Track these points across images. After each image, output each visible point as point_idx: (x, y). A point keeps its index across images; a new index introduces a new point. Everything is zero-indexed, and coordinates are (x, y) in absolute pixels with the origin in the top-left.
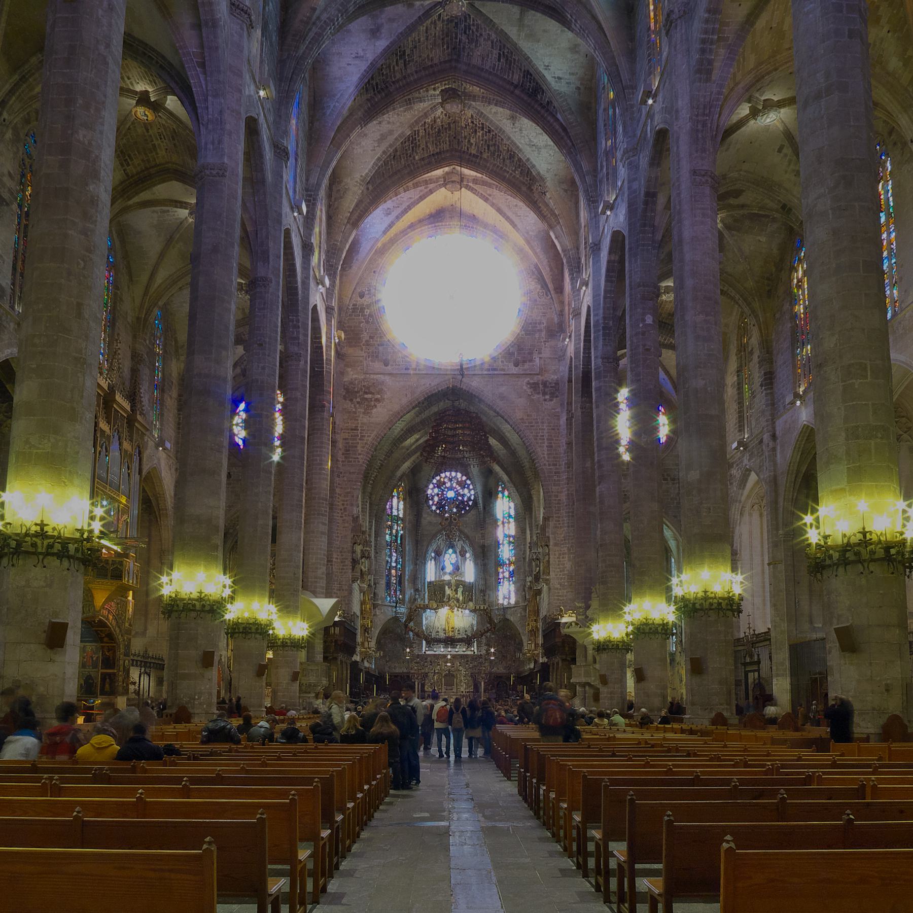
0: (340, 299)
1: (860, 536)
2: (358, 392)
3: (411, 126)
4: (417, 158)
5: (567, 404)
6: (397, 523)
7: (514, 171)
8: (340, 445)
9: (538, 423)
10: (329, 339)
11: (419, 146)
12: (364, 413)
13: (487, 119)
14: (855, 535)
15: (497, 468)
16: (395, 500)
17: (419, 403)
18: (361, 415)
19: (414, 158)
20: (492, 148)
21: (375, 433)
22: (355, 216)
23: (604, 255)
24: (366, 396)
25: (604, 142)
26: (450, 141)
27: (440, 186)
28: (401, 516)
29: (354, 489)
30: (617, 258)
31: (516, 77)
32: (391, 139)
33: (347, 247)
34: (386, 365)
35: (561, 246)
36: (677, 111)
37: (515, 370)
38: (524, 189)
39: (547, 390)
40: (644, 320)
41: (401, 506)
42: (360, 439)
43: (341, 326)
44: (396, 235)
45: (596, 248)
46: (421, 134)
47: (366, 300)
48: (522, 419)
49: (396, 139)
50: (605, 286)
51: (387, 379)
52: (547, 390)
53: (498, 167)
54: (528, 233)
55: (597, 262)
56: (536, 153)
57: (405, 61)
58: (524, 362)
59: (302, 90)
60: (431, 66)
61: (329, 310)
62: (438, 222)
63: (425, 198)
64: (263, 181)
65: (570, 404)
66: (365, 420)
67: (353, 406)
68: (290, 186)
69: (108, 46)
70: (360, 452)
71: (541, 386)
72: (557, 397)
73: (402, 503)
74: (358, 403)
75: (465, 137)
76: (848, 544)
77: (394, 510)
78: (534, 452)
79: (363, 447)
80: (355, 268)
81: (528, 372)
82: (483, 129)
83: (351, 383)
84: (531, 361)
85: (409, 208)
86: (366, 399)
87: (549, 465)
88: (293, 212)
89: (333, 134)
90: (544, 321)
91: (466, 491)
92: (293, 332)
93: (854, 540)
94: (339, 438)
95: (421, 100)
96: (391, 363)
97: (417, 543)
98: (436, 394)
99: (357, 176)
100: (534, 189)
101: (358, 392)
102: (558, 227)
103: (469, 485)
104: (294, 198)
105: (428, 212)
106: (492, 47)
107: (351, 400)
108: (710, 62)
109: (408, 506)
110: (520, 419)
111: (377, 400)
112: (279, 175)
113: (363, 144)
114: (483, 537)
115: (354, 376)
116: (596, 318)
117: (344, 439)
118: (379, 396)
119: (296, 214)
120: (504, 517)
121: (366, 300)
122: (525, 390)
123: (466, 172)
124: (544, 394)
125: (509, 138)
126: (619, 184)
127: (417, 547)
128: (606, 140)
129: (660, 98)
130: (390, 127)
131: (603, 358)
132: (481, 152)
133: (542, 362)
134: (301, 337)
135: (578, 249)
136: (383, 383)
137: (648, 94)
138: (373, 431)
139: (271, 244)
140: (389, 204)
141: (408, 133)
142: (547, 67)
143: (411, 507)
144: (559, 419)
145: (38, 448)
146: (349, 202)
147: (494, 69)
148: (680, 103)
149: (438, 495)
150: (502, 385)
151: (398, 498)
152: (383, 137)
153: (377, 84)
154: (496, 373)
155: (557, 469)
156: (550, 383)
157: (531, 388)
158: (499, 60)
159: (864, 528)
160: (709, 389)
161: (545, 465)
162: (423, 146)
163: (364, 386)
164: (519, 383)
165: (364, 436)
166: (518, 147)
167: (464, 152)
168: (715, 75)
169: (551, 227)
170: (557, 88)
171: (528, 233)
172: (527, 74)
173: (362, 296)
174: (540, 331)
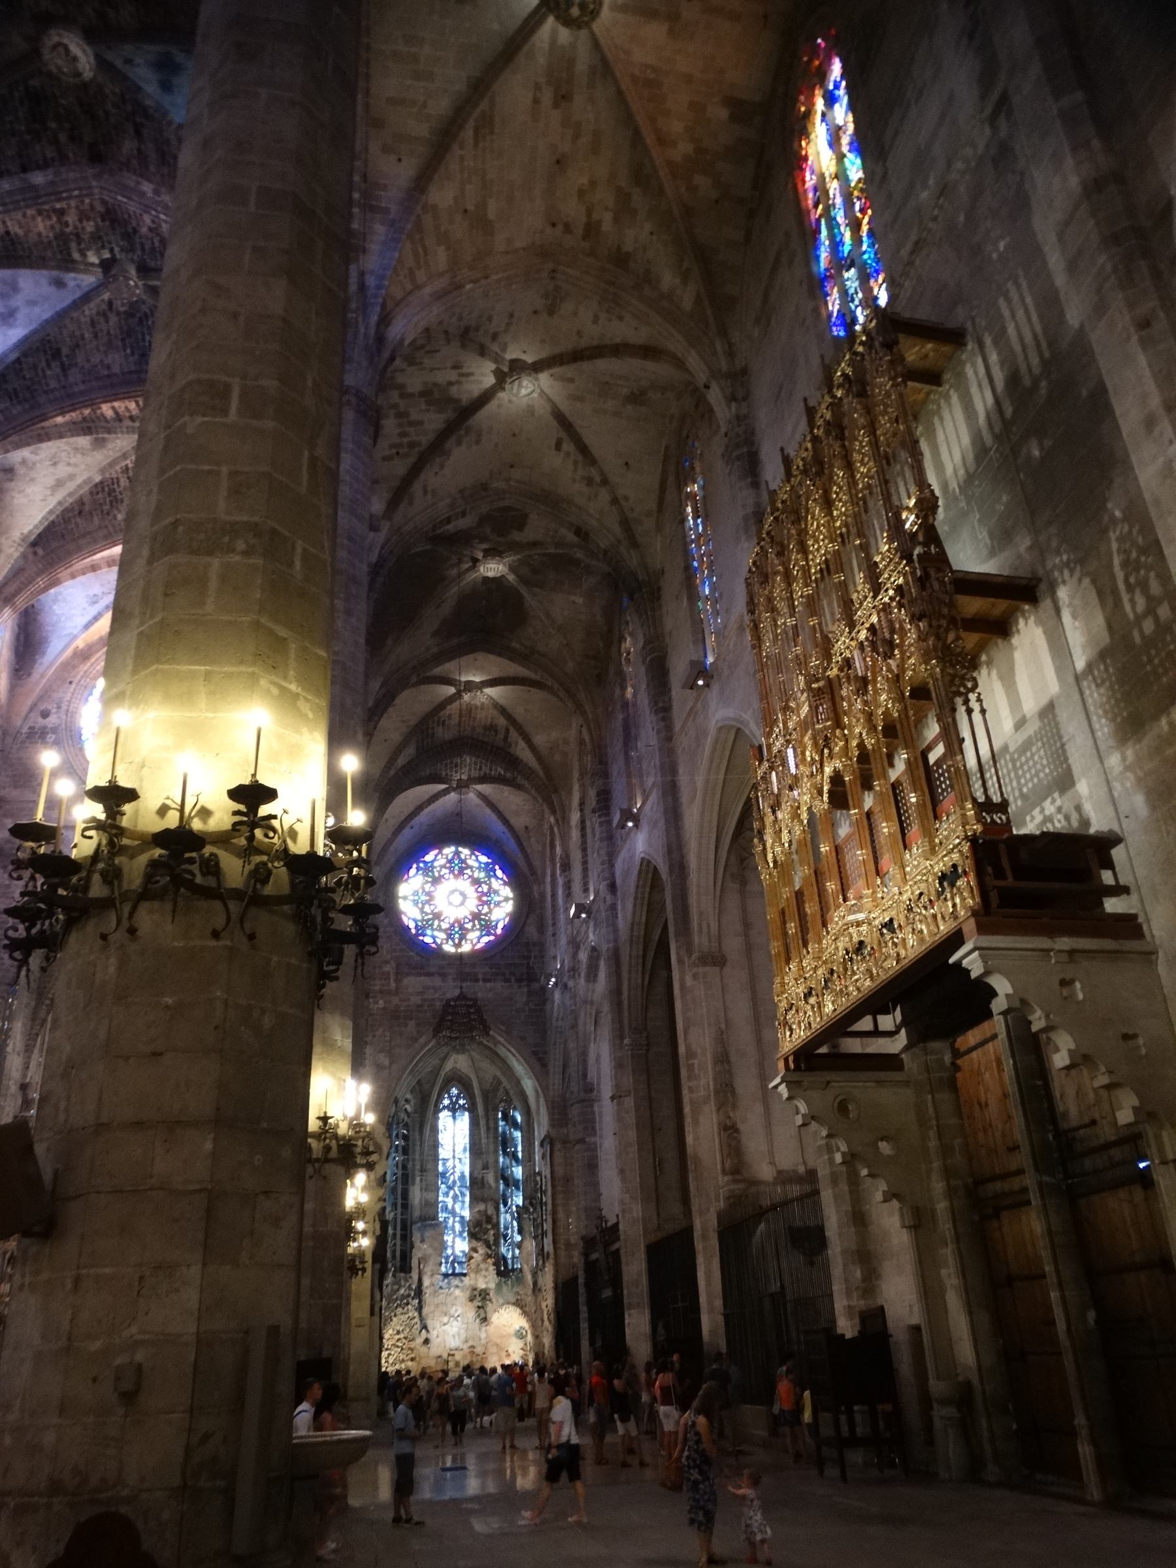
32: (71, 486)
47: (52, 720)
80: (36, 675)
99: (16, 535)
113: (29, 491)
130: (70, 470)
152: (59, 484)
173: (45, 714)
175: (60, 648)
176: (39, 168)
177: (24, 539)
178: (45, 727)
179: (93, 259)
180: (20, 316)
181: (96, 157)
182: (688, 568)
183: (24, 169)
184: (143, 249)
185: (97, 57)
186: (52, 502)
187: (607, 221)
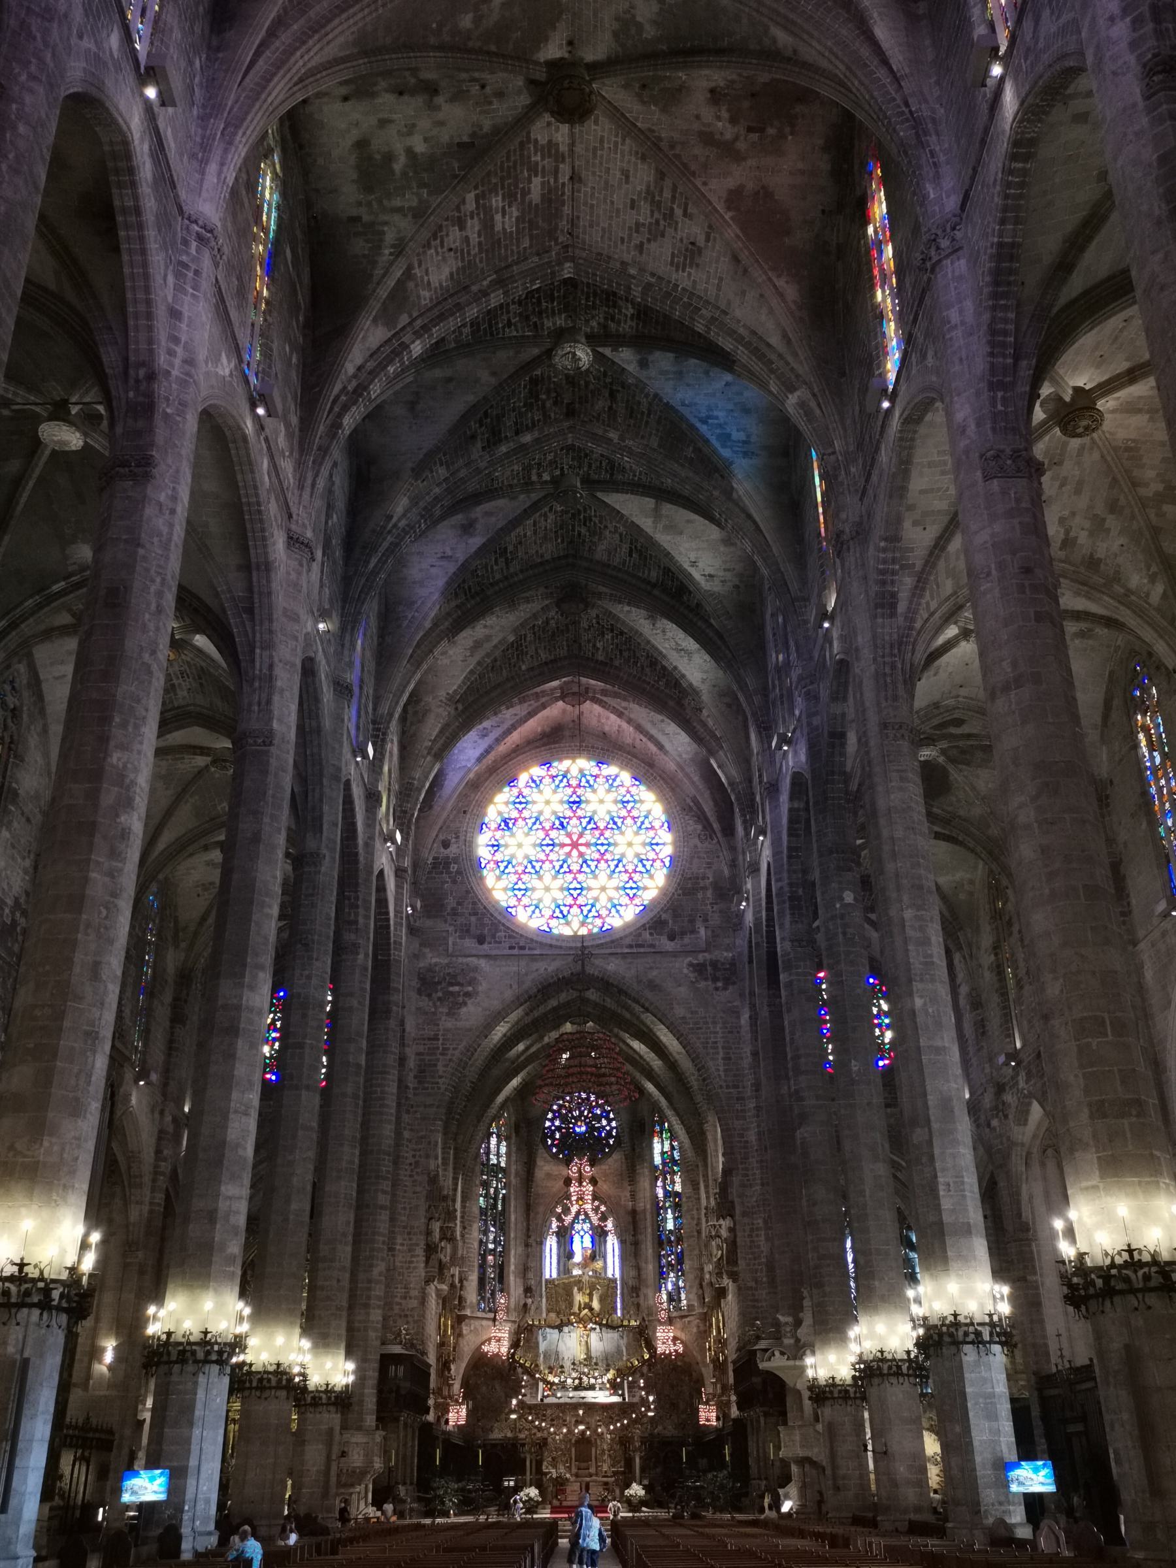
0: (416, 850)
1: (1126, 1256)
2: (439, 983)
3: (515, 631)
4: (524, 667)
5: (750, 994)
6: (496, 1177)
7: (657, 682)
8: (411, 1063)
9: (707, 1023)
10: (398, 912)
11: (527, 653)
12: (448, 1014)
13: (618, 619)
14: (1119, 1253)
15: (650, 1087)
16: (494, 1141)
17: (530, 997)
18: (443, 1018)
19: (520, 668)
20: (626, 654)
21: (464, 1043)
22: (438, 745)
23: (784, 797)
24: (451, 989)
25: (774, 655)
26: (568, 646)
27: (557, 699)
28: (503, 1165)
29: (431, 1131)
30: (802, 805)
31: (654, 574)
32: (488, 646)
33: (427, 785)
34: (481, 940)
35: (727, 778)
36: (857, 650)
37: (669, 946)
38: (671, 703)
39: (718, 974)
40: (841, 899)
41: (503, 1150)
42: (442, 1054)
43: (416, 891)
44: (494, 761)
45: (773, 789)
46: (528, 639)
47: (453, 850)
48: (684, 1018)
49: (495, 647)
50: (789, 842)
51: (482, 963)
52: (718, 974)
53: (635, 676)
54: (680, 756)
55: (775, 807)
56: (686, 660)
57: (507, 559)
58: (683, 933)
59: (371, 608)
60: (541, 564)
61: (399, 872)
62: (555, 743)
63: (536, 714)
64: (319, 730)
65: (752, 994)
66: (449, 1025)
67: (431, 1004)
68: (353, 732)
69: (153, 653)
70: (440, 1073)
72: (734, 983)
73: (504, 1143)
74: (439, 999)
75: (589, 641)
76: (1113, 1265)
79: (446, 1066)
80: (436, 809)
81: (689, 948)
82: (612, 631)
83: (430, 969)
85: (514, 727)
86: (452, 993)
87: (728, 1087)
88: (356, 756)
89: (411, 651)
90: (710, 875)
91: (604, 1122)
92: (349, 914)
93: (1119, 1260)
94: (410, 1052)
95: (527, 600)
96: (488, 939)
97: (528, 1209)
98: (554, 983)
99: (442, 694)
100: (686, 702)
101: (439, 983)
102: (721, 753)
103: (608, 1113)
104: (357, 737)
105: (539, 729)
106: (621, 541)
107: (429, 996)
108: (894, 595)
109: (514, 1149)
111: (468, 995)
112: (339, 719)
113: (451, 652)
114: (633, 1196)
115: (434, 960)
116: (780, 884)
117: (418, 1054)
118: (470, 989)
119: (359, 759)
120: (664, 1163)
121: (453, 850)
122: (686, 976)
123: (592, 682)
124: (715, 979)
125: (648, 642)
126: (797, 712)
127: (528, 1215)
128: (777, 653)
129: (838, 623)
130: (487, 631)
131: (792, 941)
132: (611, 659)
133: (710, 933)
134: (361, 920)
135: (750, 781)
136: (476, 969)
137: (825, 616)
138: (461, 1040)
139: (326, 808)
140: (486, 724)
141: (511, 638)
142: (694, 564)
143: (519, 1149)
144: (738, 1018)
145: (25, 1156)
146: (431, 729)
147: (624, 565)
148: (860, 639)
149: (559, 1129)
150: (651, 968)
151: (498, 1136)
152: (477, 645)
153: (470, 588)
154: (642, 950)
155: (739, 1092)
156: (723, 964)
157: (694, 972)
158: (631, 555)
159: (1129, 1245)
160: (930, 1010)
161: (721, 1087)
162: (532, 651)
163: (449, 974)
164: (677, 965)
165: (448, 1049)
166: (661, 653)
167: (588, 659)
168: (902, 607)
169: (711, 753)
170: (708, 588)
171: (680, 756)
172: (667, 571)
173: (446, 844)
174: (704, 888)
175: (456, 781)
176: (528, 428)
177: (450, 698)
179: (546, 477)
180: (478, 526)
181: (570, 413)
182: (1145, 793)
183: (517, 433)
184: (590, 466)
185: (593, 351)
186: (472, 663)
187: (1083, 538)
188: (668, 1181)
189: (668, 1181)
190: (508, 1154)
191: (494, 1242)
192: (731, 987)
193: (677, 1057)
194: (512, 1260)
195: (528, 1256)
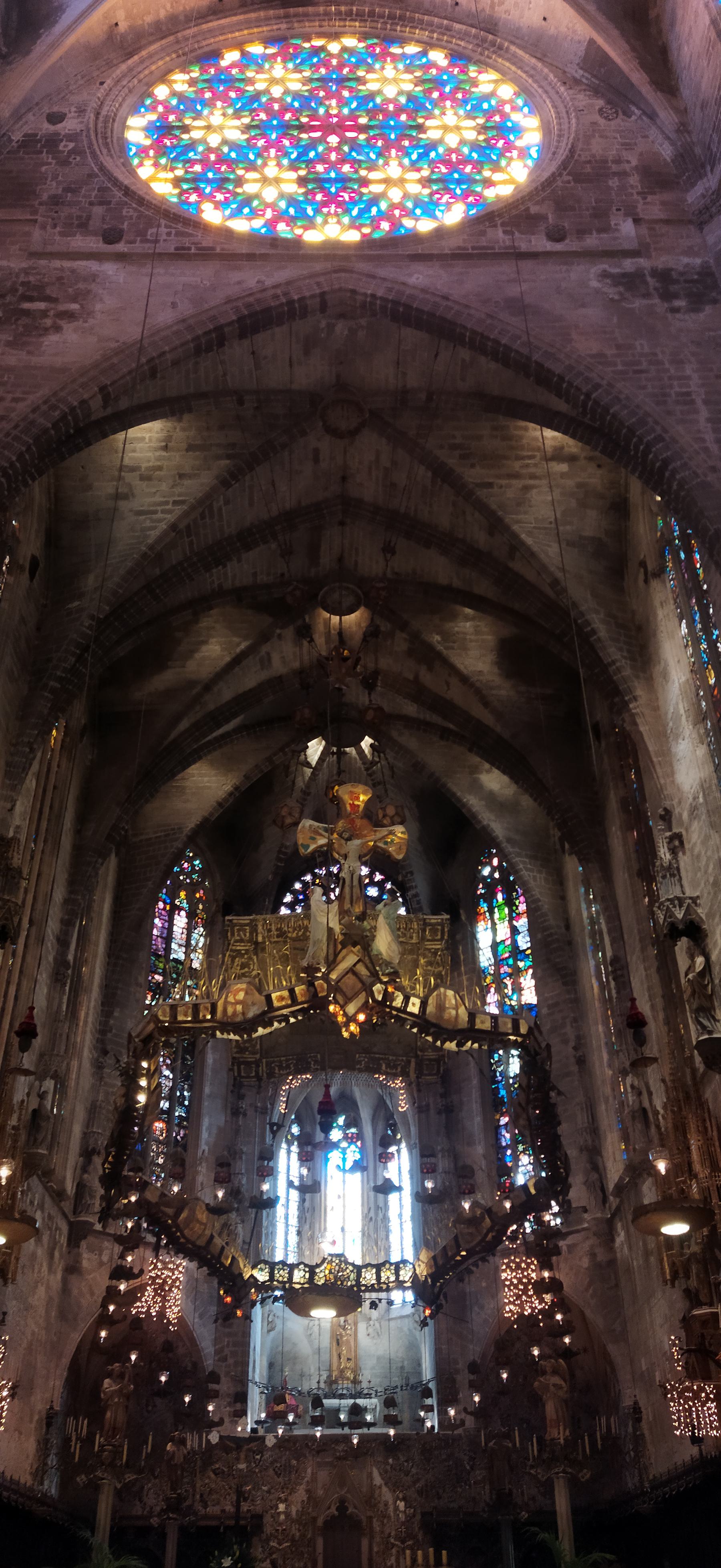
16: (180, 921)
37: (550, 246)
39: (673, 288)
47: (70, 125)
48: (601, 355)
52: (673, 288)
58: (581, 233)
71: (649, 279)
72: (715, 302)
77: (174, 946)
78: (660, 439)
84: (600, 231)
86: (27, 313)
110: (592, 356)
122: (597, 291)
124: (667, 296)
151: (191, 915)
156: (682, 274)
157: (615, 284)
173: (55, 118)
174: (623, 174)
178: (57, 134)
188: (509, 991)
189: (509, 991)
190: (209, 951)
191: (170, 1098)
192: (708, 309)
193: (559, 575)
194: (205, 1135)
195: (237, 1132)
